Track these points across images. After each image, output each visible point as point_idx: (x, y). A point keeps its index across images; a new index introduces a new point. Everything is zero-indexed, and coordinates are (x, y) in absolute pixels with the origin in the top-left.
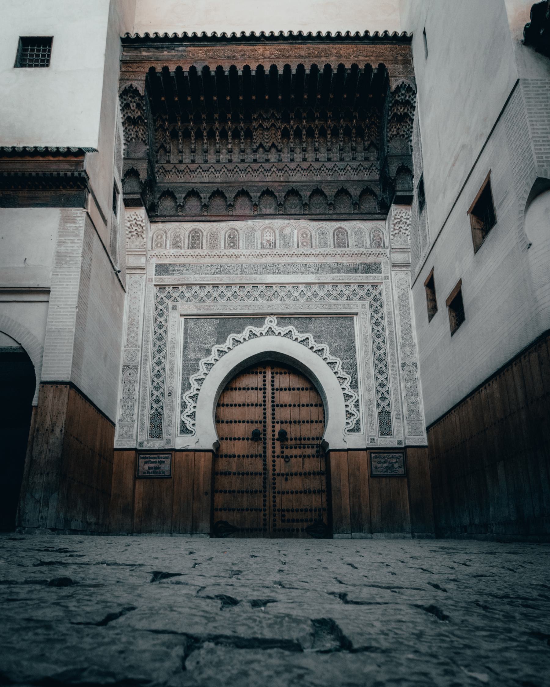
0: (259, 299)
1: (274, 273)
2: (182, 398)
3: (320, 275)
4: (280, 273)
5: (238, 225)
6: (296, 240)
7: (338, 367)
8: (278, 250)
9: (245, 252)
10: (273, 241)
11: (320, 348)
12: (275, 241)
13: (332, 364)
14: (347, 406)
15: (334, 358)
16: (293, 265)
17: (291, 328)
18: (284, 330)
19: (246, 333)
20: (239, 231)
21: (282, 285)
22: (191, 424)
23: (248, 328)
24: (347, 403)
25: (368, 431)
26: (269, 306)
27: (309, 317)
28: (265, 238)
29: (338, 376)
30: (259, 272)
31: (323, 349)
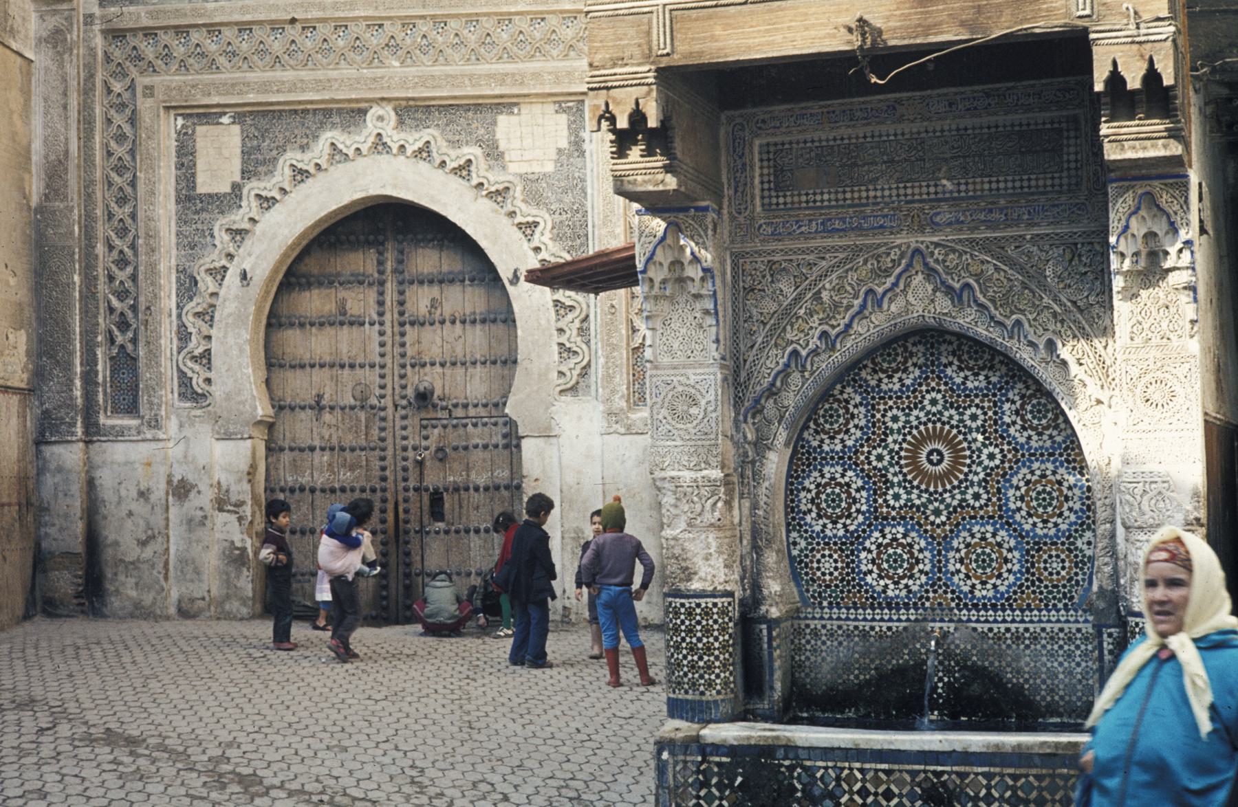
2: (179, 316)
18: (415, 139)
19: (321, 149)
22: (200, 381)
23: (328, 136)
24: (561, 324)
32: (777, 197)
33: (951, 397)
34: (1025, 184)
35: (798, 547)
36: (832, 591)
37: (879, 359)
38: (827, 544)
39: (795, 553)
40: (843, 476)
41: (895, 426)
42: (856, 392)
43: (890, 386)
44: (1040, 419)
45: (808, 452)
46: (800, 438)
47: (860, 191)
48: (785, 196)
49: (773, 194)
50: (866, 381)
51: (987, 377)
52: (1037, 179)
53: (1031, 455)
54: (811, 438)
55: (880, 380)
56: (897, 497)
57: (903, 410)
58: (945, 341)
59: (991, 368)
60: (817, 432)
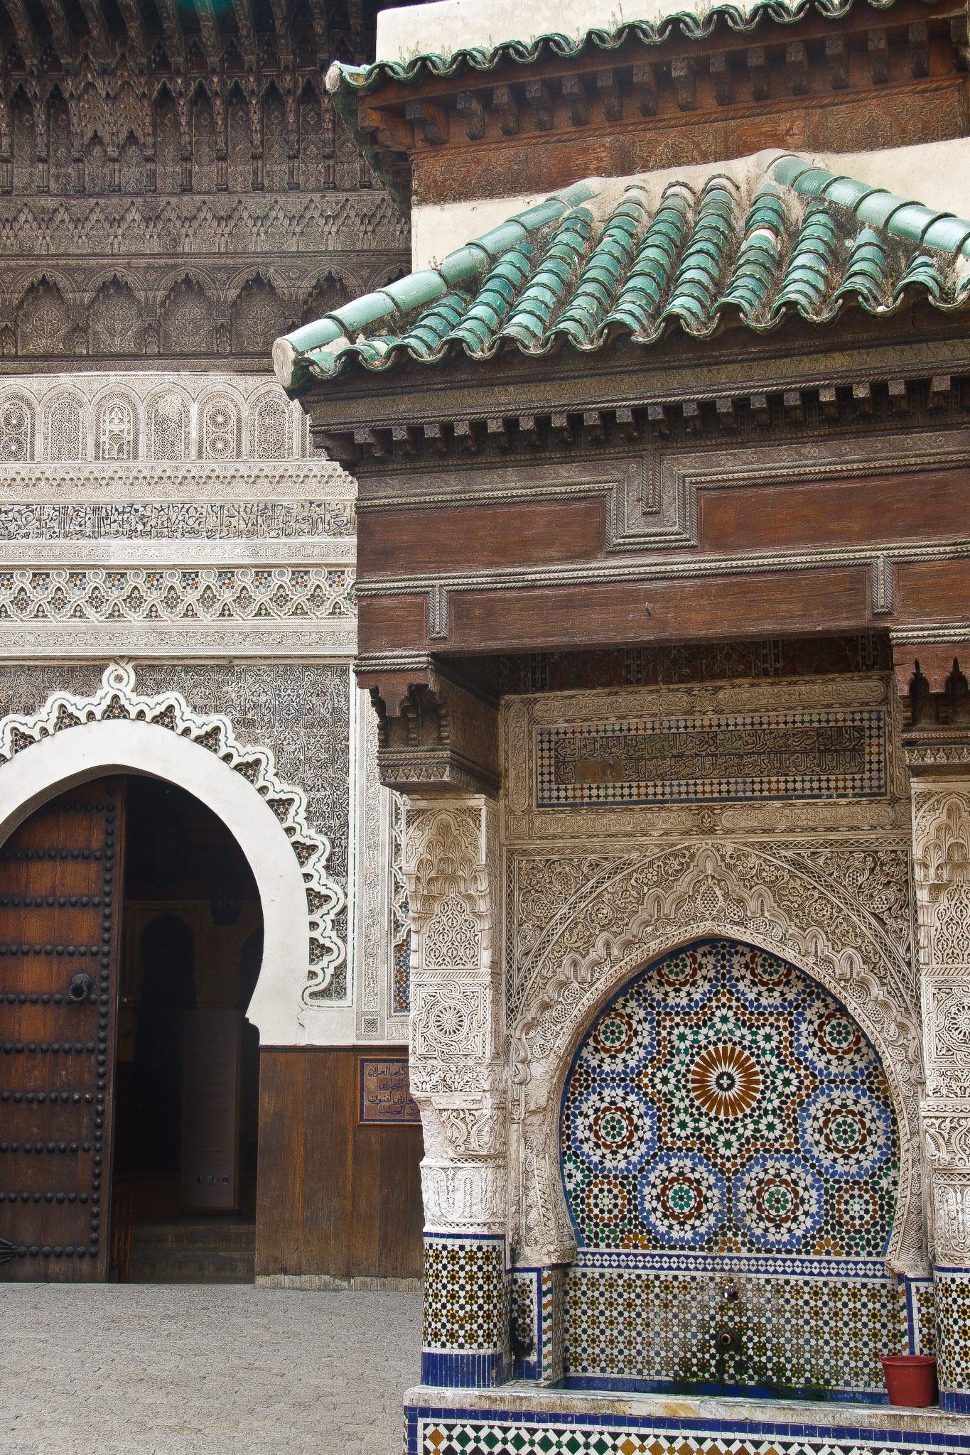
0: (89, 611)
1: (131, 534)
3: (260, 541)
4: (145, 534)
5: (33, 385)
6: (194, 435)
7: (297, 815)
8: (143, 465)
9: (49, 469)
10: (131, 438)
11: (250, 759)
12: (136, 441)
13: (280, 806)
14: (313, 925)
15: (286, 787)
16: (185, 507)
17: (171, 697)
18: (155, 703)
19: (47, 713)
20: (35, 404)
21: (153, 574)
23: (58, 697)
24: (316, 917)
25: (359, 999)
26: (112, 635)
27: (227, 666)
28: (107, 427)
29: (294, 839)
30: (88, 531)
31: (258, 762)
32: (558, 790)
33: (743, 1014)
34: (824, 784)
35: (574, 1180)
36: (611, 1231)
37: (665, 971)
38: (605, 1177)
39: (570, 1186)
40: (624, 1100)
41: (682, 1046)
42: (640, 1006)
43: (677, 1000)
44: (840, 1042)
45: (586, 1072)
46: (578, 1056)
47: (647, 787)
48: (566, 790)
49: (554, 786)
50: (651, 994)
51: (782, 994)
52: (837, 780)
53: (831, 1081)
54: (590, 1057)
55: (666, 994)
56: (683, 1125)
57: (691, 1027)
58: (737, 952)
59: (787, 983)
60: (596, 1050)
